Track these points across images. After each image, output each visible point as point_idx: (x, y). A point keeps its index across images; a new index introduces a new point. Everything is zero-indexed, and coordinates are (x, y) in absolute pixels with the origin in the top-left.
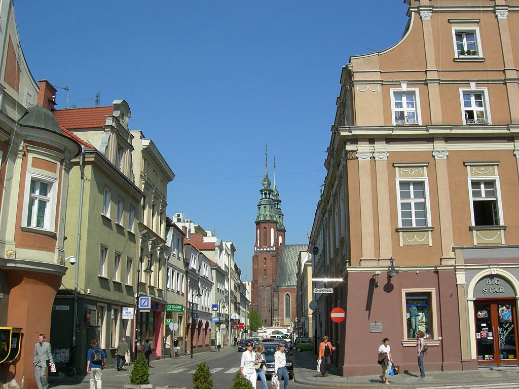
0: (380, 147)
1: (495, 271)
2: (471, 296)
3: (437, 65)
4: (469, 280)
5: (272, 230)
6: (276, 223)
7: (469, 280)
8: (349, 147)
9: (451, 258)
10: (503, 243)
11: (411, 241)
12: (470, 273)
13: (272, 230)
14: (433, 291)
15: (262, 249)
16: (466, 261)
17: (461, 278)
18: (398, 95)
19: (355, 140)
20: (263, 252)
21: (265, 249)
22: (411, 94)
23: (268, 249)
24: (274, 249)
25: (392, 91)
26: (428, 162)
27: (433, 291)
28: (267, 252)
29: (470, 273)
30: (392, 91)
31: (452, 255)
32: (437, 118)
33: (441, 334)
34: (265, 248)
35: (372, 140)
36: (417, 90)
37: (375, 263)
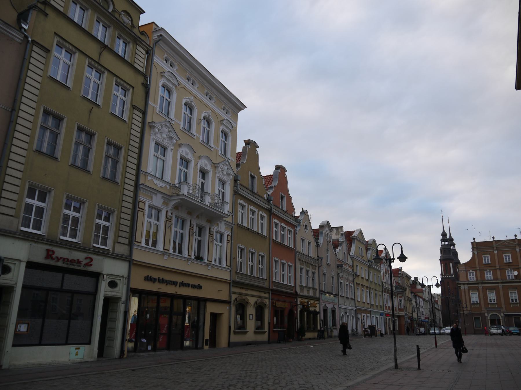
0: (466, 286)
1: (494, 313)
2: (489, 318)
3: (479, 266)
4: (488, 315)
5: (451, 264)
6: (453, 260)
7: (488, 315)
8: (459, 286)
9: (484, 310)
10: (496, 307)
11: (475, 306)
12: (488, 314)
13: (451, 264)
14: (480, 317)
15: (445, 277)
16: (487, 311)
17: (486, 315)
18: (470, 273)
19: (460, 284)
20: (447, 278)
21: (448, 277)
22: (473, 273)
23: (450, 276)
24: (454, 276)
25: (468, 272)
26: (477, 289)
27: (480, 317)
28: (449, 278)
29: (488, 314)
30: (468, 272)
31: (484, 309)
32: (479, 278)
33: (482, 326)
34: (448, 275)
35: (464, 284)
36: (474, 272)
37: (466, 311)
